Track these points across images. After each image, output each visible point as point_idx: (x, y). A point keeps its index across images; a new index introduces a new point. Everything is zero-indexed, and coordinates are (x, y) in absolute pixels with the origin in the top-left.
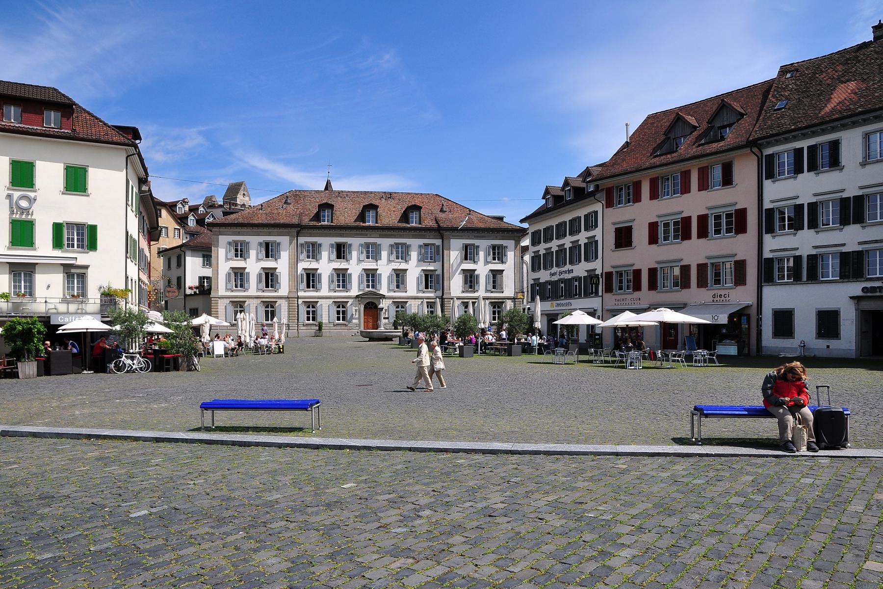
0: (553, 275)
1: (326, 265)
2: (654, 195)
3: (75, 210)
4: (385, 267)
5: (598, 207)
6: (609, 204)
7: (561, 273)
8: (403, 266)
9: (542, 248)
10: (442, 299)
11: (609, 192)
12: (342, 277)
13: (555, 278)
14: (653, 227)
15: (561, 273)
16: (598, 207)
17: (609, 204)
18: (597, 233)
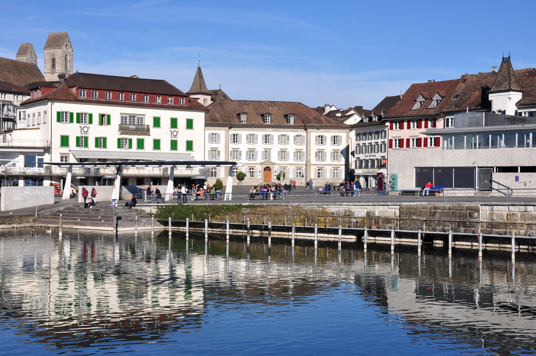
0: (366, 156)
1: (243, 146)
2: (409, 127)
4: (275, 148)
5: (386, 129)
7: (370, 156)
10: (306, 165)
12: (251, 153)
13: (367, 158)
15: (370, 156)
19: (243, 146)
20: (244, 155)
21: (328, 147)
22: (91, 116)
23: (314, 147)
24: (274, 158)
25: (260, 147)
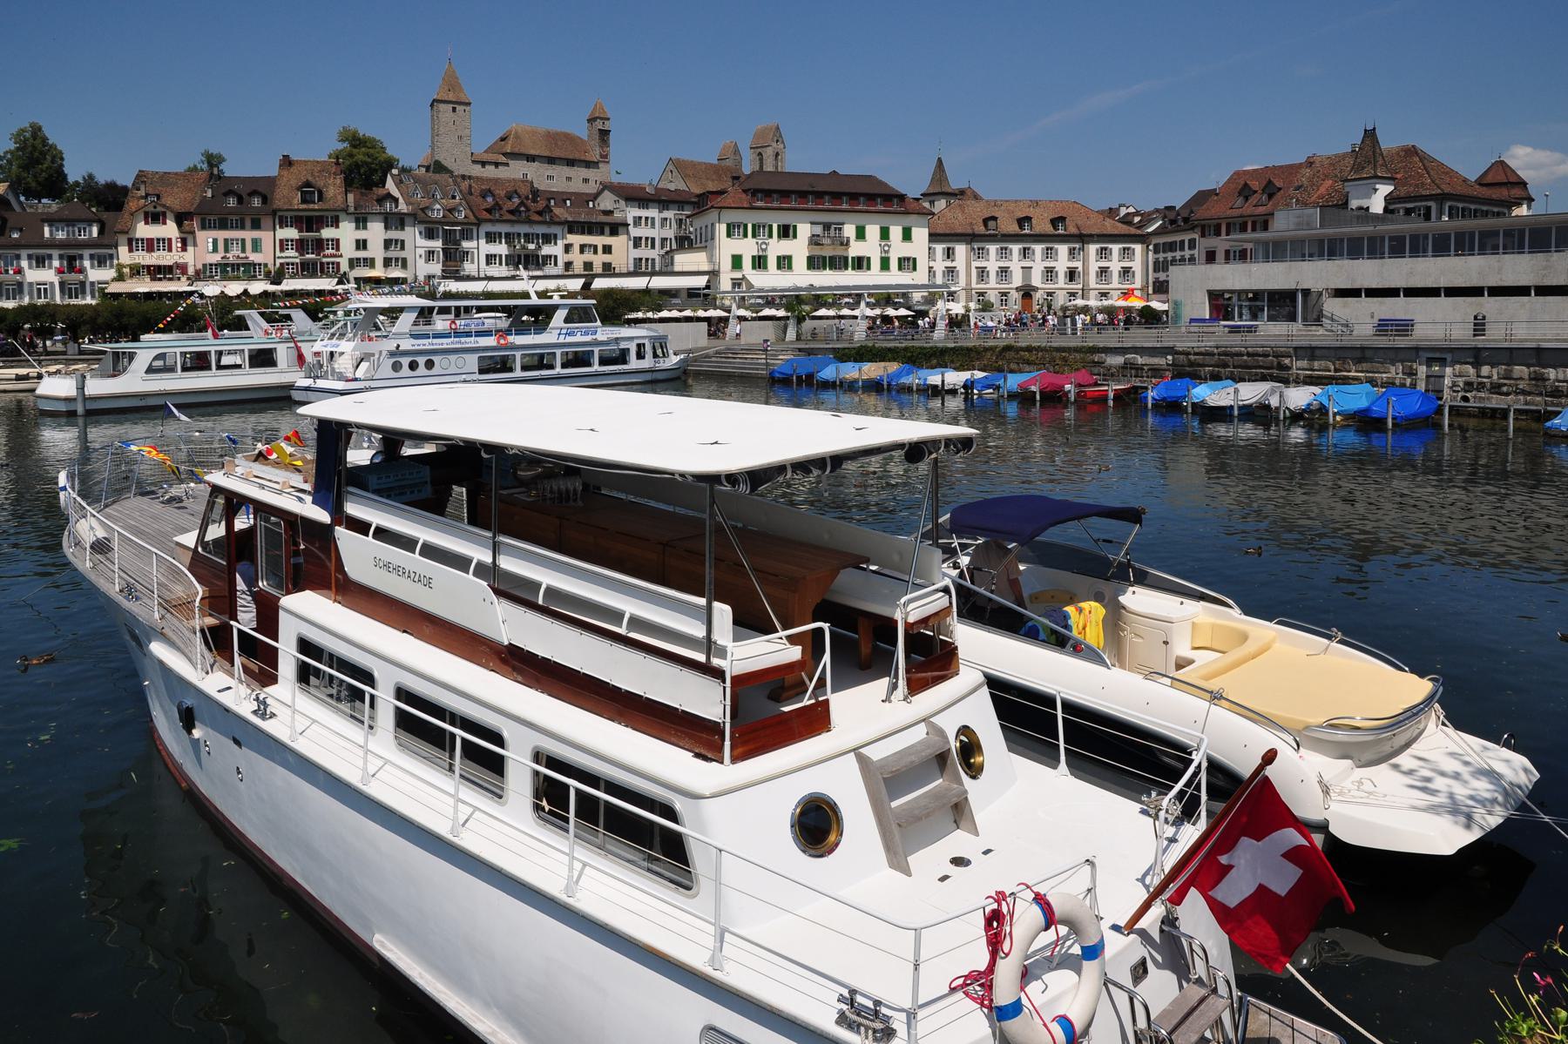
3: (905, 250)
4: (1038, 265)
6: (1203, 235)
8: (1052, 264)
9: (1161, 256)
11: (1203, 227)
14: (1227, 252)
16: (1196, 236)
17: (1203, 235)
18: (1196, 252)
19: (993, 264)
20: (993, 276)
21: (1115, 265)
23: (1094, 265)
24: (1037, 280)
25: (1015, 264)
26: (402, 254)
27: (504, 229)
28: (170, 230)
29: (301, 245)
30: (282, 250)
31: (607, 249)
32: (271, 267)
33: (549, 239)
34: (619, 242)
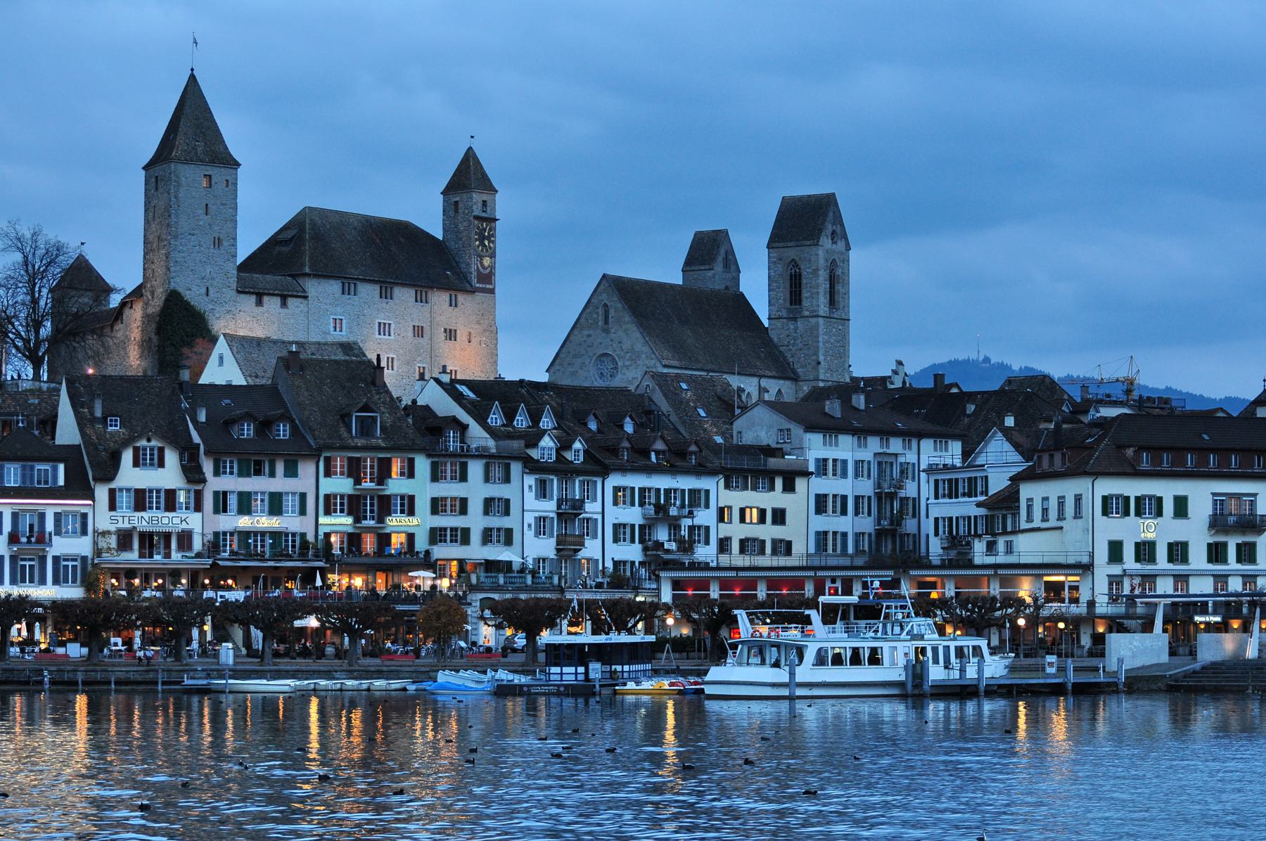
22: (1160, 500)
26: (505, 522)
27: (637, 481)
28: (169, 476)
29: (354, 505)
30: (328, 512)
31: (779, 517)
32: (310, 538)
33: (697, 499)
34: (797, 503)
